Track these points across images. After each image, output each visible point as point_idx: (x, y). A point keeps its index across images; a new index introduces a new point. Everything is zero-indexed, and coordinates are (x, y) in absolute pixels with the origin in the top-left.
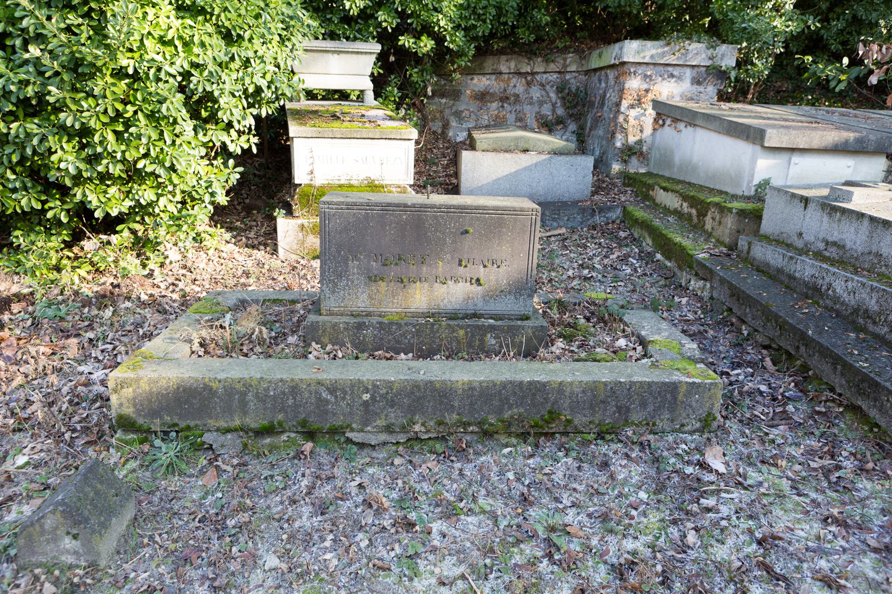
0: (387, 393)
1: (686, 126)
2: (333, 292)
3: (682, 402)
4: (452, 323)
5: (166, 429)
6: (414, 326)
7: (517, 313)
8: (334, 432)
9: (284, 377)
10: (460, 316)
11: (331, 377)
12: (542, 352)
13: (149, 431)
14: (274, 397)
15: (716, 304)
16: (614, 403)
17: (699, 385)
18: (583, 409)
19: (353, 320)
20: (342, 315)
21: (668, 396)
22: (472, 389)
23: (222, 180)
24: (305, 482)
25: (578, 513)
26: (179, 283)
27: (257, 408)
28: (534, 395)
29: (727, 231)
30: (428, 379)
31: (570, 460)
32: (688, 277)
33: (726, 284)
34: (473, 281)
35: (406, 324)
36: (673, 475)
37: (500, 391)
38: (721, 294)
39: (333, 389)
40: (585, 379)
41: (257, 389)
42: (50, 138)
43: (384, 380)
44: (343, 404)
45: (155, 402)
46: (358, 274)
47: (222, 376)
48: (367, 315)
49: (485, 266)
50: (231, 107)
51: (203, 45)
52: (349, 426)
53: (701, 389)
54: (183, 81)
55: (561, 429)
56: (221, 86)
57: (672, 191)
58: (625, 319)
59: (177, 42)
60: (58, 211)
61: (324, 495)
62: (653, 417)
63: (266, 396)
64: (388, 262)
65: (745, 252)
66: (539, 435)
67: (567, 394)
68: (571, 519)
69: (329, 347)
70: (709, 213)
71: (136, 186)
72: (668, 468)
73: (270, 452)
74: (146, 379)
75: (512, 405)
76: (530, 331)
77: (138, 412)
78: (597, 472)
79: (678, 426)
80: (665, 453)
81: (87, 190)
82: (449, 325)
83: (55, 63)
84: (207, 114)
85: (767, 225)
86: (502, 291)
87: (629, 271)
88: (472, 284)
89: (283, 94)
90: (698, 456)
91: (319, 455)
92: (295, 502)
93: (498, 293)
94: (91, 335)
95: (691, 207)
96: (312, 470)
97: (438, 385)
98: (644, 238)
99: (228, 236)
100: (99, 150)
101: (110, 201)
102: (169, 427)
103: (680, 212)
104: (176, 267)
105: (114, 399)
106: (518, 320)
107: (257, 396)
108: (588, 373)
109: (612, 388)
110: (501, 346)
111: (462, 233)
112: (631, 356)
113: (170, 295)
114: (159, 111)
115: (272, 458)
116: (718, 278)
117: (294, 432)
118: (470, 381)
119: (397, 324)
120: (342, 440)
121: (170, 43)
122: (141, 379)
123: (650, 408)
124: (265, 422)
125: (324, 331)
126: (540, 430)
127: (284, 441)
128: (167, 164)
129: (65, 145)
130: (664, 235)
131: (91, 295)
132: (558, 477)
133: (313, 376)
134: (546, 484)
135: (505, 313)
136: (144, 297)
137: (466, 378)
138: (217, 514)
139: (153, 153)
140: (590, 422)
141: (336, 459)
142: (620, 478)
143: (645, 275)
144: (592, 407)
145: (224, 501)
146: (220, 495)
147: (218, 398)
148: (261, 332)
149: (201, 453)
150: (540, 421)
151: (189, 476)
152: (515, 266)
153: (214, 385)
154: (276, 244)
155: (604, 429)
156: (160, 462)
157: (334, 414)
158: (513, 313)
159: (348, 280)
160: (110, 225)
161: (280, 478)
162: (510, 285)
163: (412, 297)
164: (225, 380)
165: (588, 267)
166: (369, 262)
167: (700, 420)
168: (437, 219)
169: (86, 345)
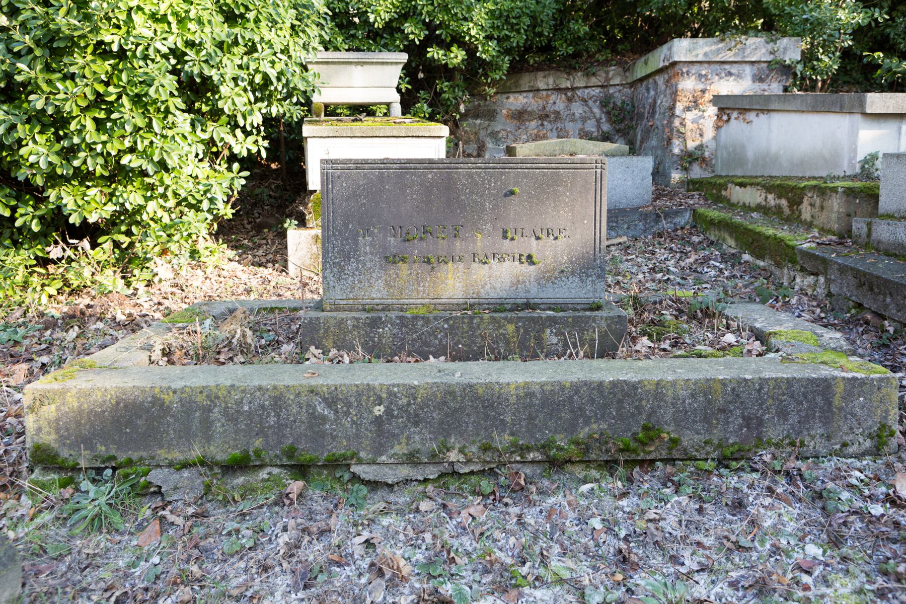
0: (409, 404)
1: (757, 115)
2: (339, 279)
3: (841, 409)
4: (495, 315)
5: (98, 464)
6: (446, 320)
7: (585, 301)
8: (335, 464)
9: (264, 383)
10: (508, 307)
11: (329, 382)
12: (622, 350)
13: (76, 469)
14: (250, 415)
15: (838, 300)
16: (738, 412)
17: (863, 382)
18: (694, 422)
19: (364, 315)
20: (351, 310)
21: (819, 399)
22: (530, 395)
23: (225, 183)
24: (284, 538)
25: (713, 582)
26: (165, 301)
27: (225, 431)
28: (620, 402)
29: (834, 216)
30: (466, 381)
31: (684, 500)
32: (792, 273)
33: (849, 273)
34: (524, 259)
35: (435, 318)
36: (851, 518)
37: (571, 397)
38: (844, 287)
39: (331, 401)
40: (693, 376)
41: (226, 403)
42: (19, 126)
43: (404, 385)
44: (346, 422)
45: (85, 424)
46: (371, 253)
47: (178, 385)
48: (383, 310)
49: (538, 238)
50: (233, 98)
51: (200, 22)
52: (354, 455)
53: (866, 388)
54: (177, 64)
55: (664, 454)
56: (222, 70)
57: (751, 184)
58: (727, 312)
59: (171, 18)
60: (29, 218)
61: (311, 558)
62: (799, 433)
63: (238, 412)
64: (410, 237)
65: (864, 236)
66: (631, 464)
67: (668, 399)
68: (704, 592)
69: (334, 352)
70: (806, 198)
71: (120, 188)
72: (841, 508)
73: (243, 497)
74: (74, 392)
75: (590, 418)
76: (604, 324)
77: (61, 439)
78: (729, 517)
79: (838, 447)
80: (830, 485)
81: (62, 192)
82: (494, 318)
83: (27, 37)
84: (208, 108)
85: (886, 203)
86: (562, 271)
87: (713, 273)
88: (522, 263)
89: (294, 89)
90: (883, 489)
91: (311, 499)
92: (266, 569)
93: (556, 274)
94: (45, 359)
95: (780, 197)
96: (299, 521)
97: (480, 391)
98: (724, 240)
99: (231, 253)
100: (76, 140)
101: (89, 204)
102: (103, 462)
103: (765, 207)
104: (166, 287)
105: (30, 422)
106: (585, 310)
107: (225, 412)
108: (695, 370)
109: (733, 389)
110: (566, 345)
111: (506, 195)
112: (749, 351)
113: (152, 313)
114: (146, 94)
115: (244, 506)
116: (836, 266)
117: (276, 466)
118: (526, 383)
119: (423, 318)
120: (347, 477)
121: (163, 19)
122: (68, 390)
123: (794, 419)
124: (237, 453)
125: (326, 331)
126: (633, 457)
127: (263, 480)
128: (156, 158)
129: (37, 137)
130: (750, 230)
131: (57, 315)
132: (670, 523)
133: (304, 382)
134: (652, 534)
135: (568, 301)
136: (120, 317)
137: (521, 380)
138: (146, 590)
139: (140, 147)
140: (705, 443)
141: (336, 506)
142: (766, 525)
143: (734, 276)
144: (706, 419)
145: (160, 568)
146: (156, 559)
147: (172, 416)
148: (244, 335)
149: (144, 500)
150: (633, 444)
151: (122, 534)
152: (578, 237)
153: (167, 398)
154: (286, 261)
155: (728, 453)
156: (83, 513)
157: (334, 438)
158: (578, 301)
159: (358, 262)
160: (92, 232)
161: (250, 533)
162: (572, 263)
163: (443, 282)
164: (183, 390)
165: (661, 271)
166: (385, 237)
167: (870, 436)
168: (472, 178)
169: (36, 370)
